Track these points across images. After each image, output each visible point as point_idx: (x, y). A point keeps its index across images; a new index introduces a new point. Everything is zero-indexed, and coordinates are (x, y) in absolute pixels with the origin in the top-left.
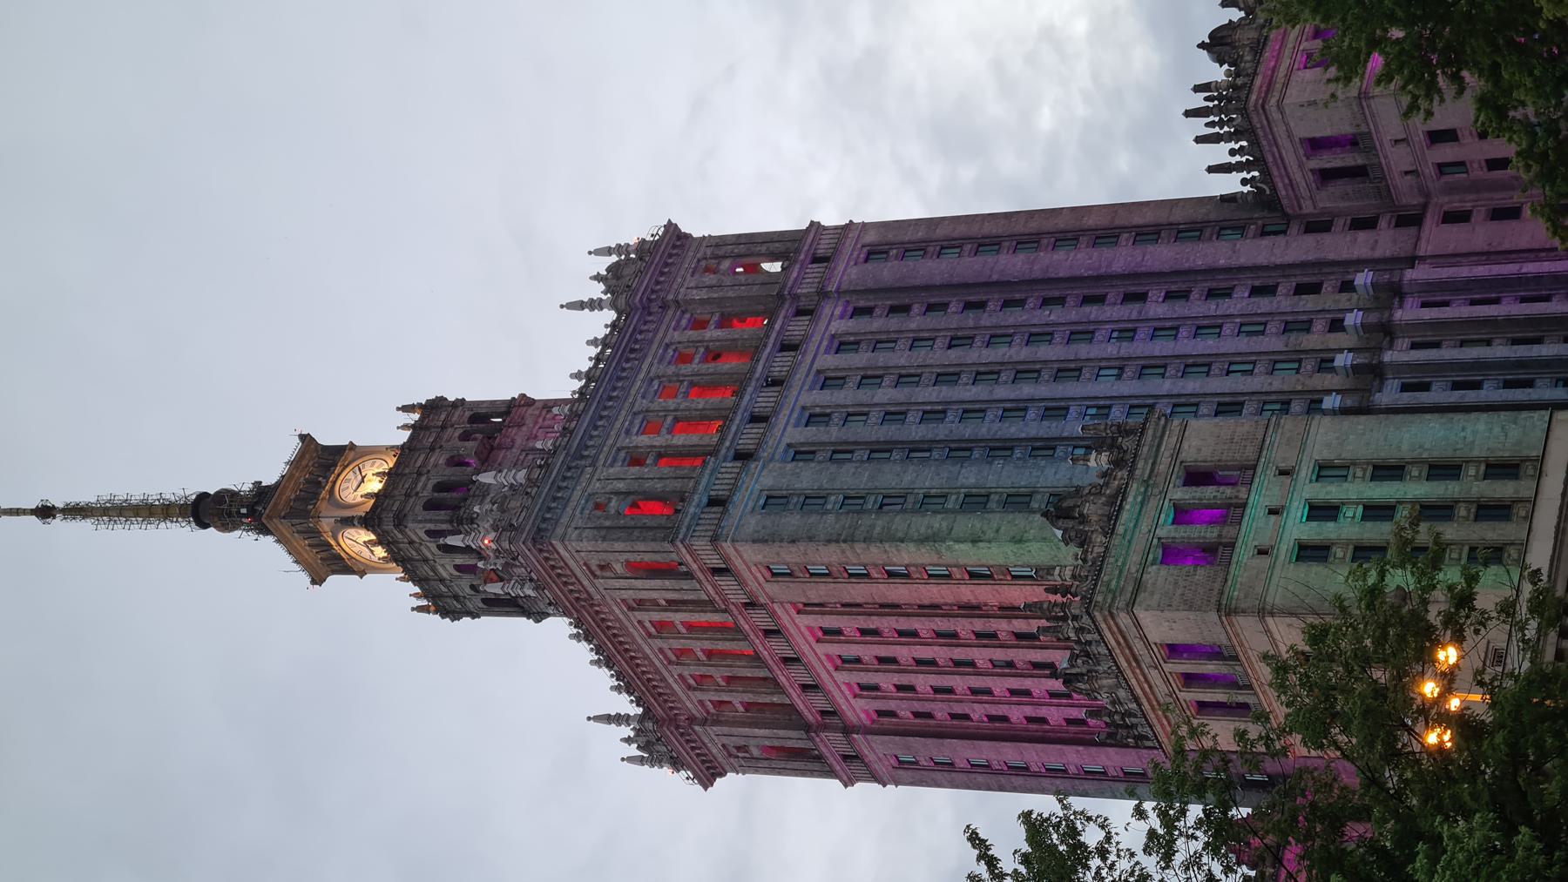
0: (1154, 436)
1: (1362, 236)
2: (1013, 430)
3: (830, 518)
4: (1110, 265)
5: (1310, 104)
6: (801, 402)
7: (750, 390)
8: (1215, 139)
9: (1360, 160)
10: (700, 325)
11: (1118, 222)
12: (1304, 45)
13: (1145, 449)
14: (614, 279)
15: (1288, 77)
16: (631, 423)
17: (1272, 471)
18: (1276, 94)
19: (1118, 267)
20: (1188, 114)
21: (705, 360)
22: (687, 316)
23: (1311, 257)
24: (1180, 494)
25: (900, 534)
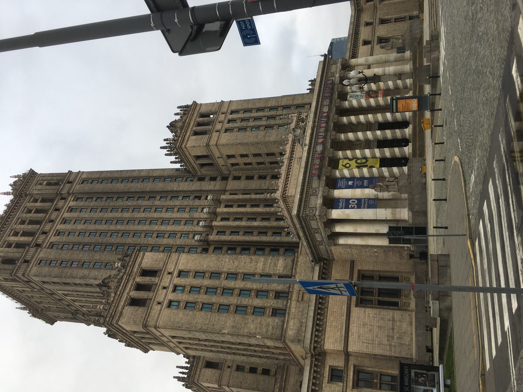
0: (134, 258)
1: (212, 182)
2: (113, 240)
8: (170, 155)
9: (210, 162)
10: (36, 201)
11: (150, 175)
12: (194, 128)
13: (131, 263)
14: (14, 185)
15: (188, 138)
16: (11, 232)
20: (161, 148)
21: (35, 212)
23: (198, 189)
24: (139, 280)
25: (75, 276)
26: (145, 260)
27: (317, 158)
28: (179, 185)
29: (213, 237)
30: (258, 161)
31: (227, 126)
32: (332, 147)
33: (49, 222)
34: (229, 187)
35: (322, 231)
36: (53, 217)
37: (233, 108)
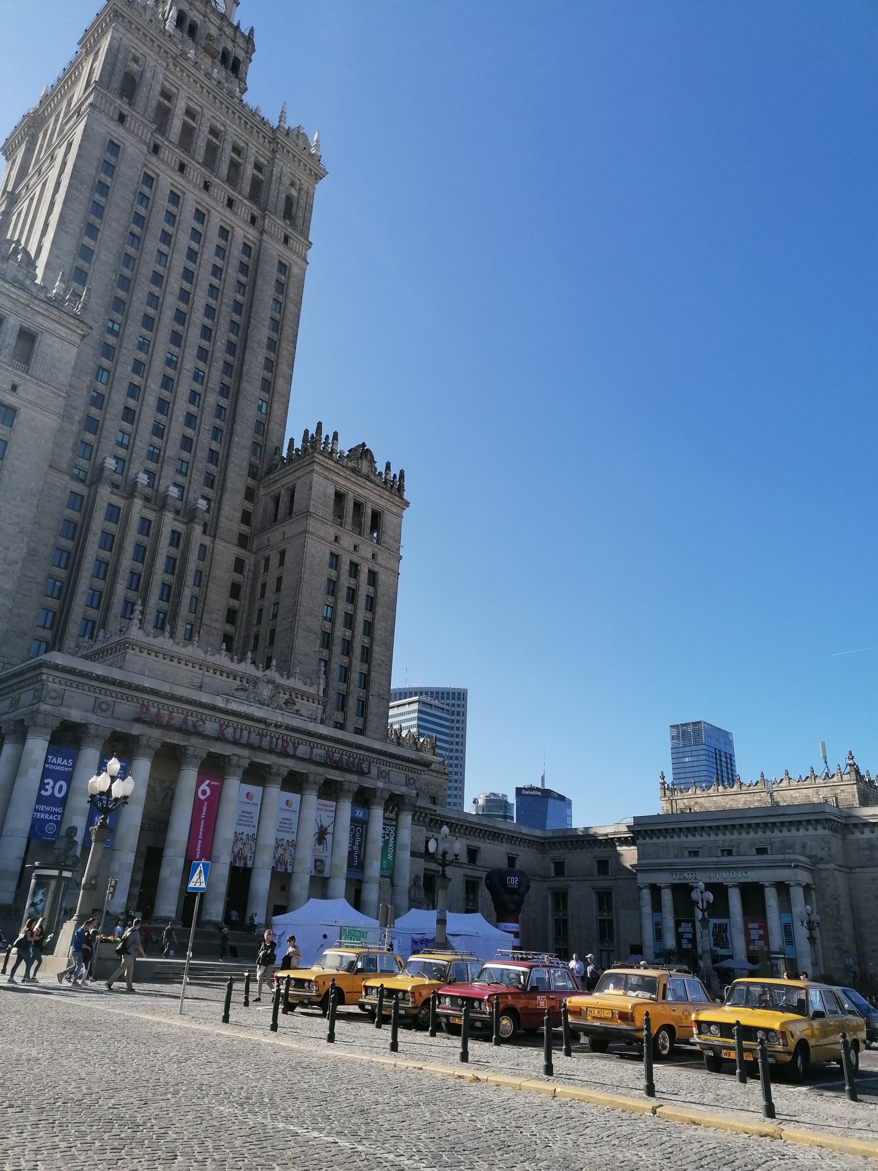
1: (238, 515)
3: (93, 172)
4: (247, 381)
5: (311, 487)
6: (187, 192)
7: (204, 170)
8: (305, 440)
10: (258, 167)
12: (351, 495)
13: (57, 313)
14: (299, 135)
15: (332, 480)
16: (197, 104)
17: (17, 380)
18: (321, 471)
19: (244, 385)
20: (319, 425)
22: (266, 163)
23: (229, 485)
25: (69, 204)
26: (58, 344)
27: (185, 721)
28: (242, 448)
29: (105, 495)
30: (264, 611)
31: (345, 560)
32: (210, 755)
33: (206, 182)
34: (220, 545)
35: (11, 715)
36: (214, 190)
37: (382, 577)
